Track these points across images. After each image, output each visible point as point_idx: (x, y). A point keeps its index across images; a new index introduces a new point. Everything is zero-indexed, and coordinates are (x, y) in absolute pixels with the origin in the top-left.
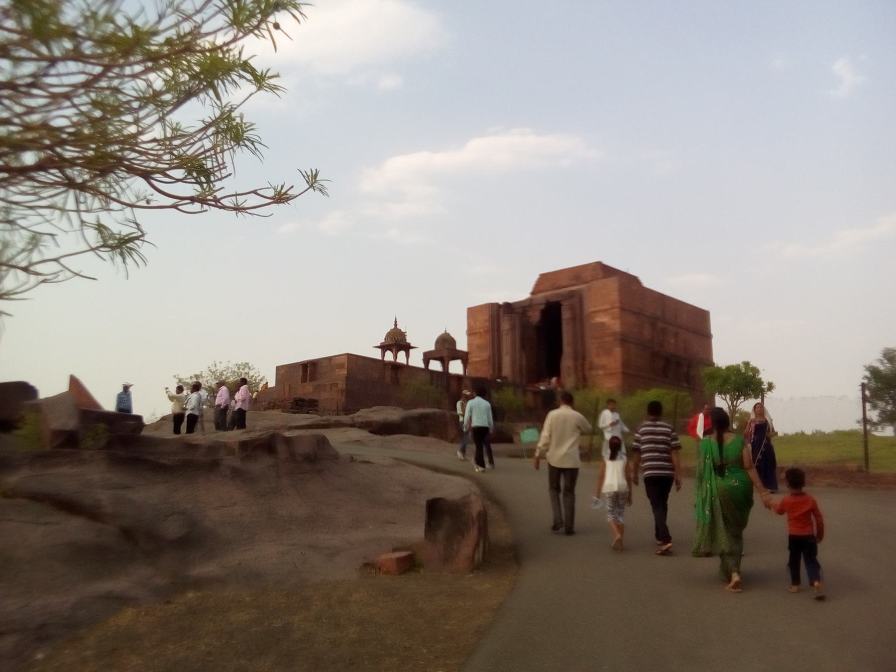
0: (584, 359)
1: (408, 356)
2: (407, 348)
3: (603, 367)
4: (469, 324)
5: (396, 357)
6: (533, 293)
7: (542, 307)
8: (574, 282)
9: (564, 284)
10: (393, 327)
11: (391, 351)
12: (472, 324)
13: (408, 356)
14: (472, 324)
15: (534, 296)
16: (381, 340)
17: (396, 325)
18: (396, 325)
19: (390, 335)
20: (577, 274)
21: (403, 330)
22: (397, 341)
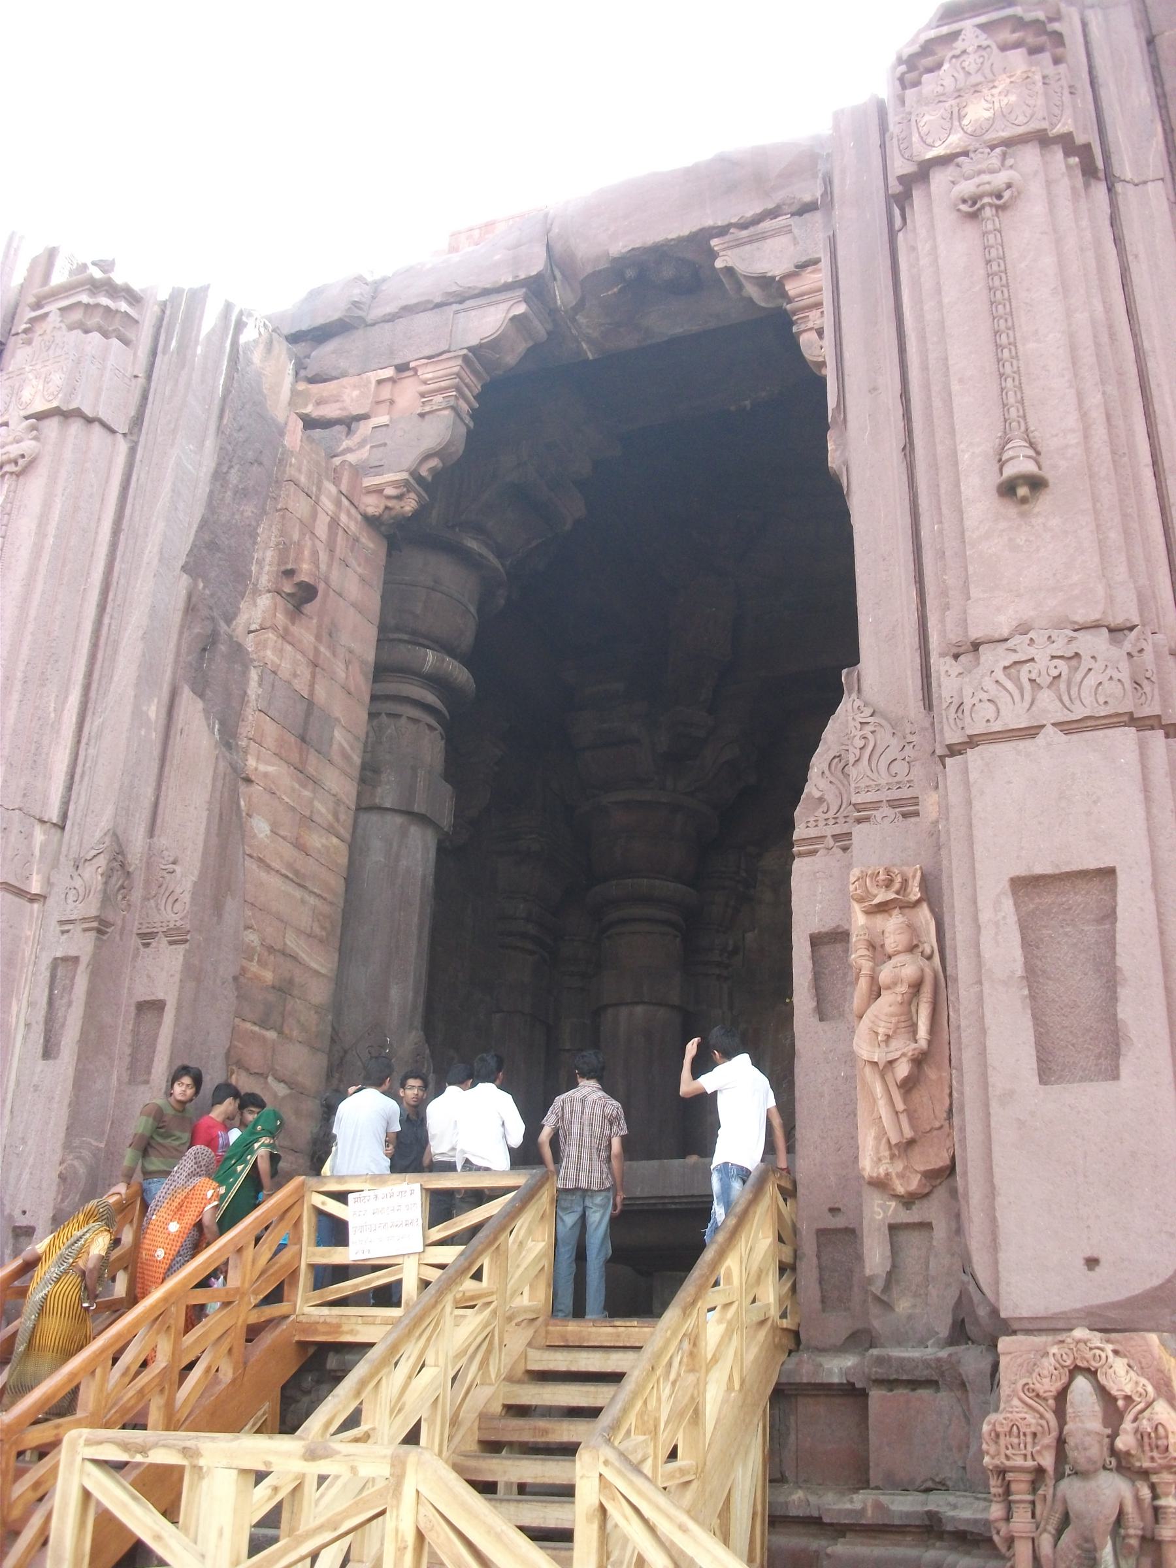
7: (487, 322)
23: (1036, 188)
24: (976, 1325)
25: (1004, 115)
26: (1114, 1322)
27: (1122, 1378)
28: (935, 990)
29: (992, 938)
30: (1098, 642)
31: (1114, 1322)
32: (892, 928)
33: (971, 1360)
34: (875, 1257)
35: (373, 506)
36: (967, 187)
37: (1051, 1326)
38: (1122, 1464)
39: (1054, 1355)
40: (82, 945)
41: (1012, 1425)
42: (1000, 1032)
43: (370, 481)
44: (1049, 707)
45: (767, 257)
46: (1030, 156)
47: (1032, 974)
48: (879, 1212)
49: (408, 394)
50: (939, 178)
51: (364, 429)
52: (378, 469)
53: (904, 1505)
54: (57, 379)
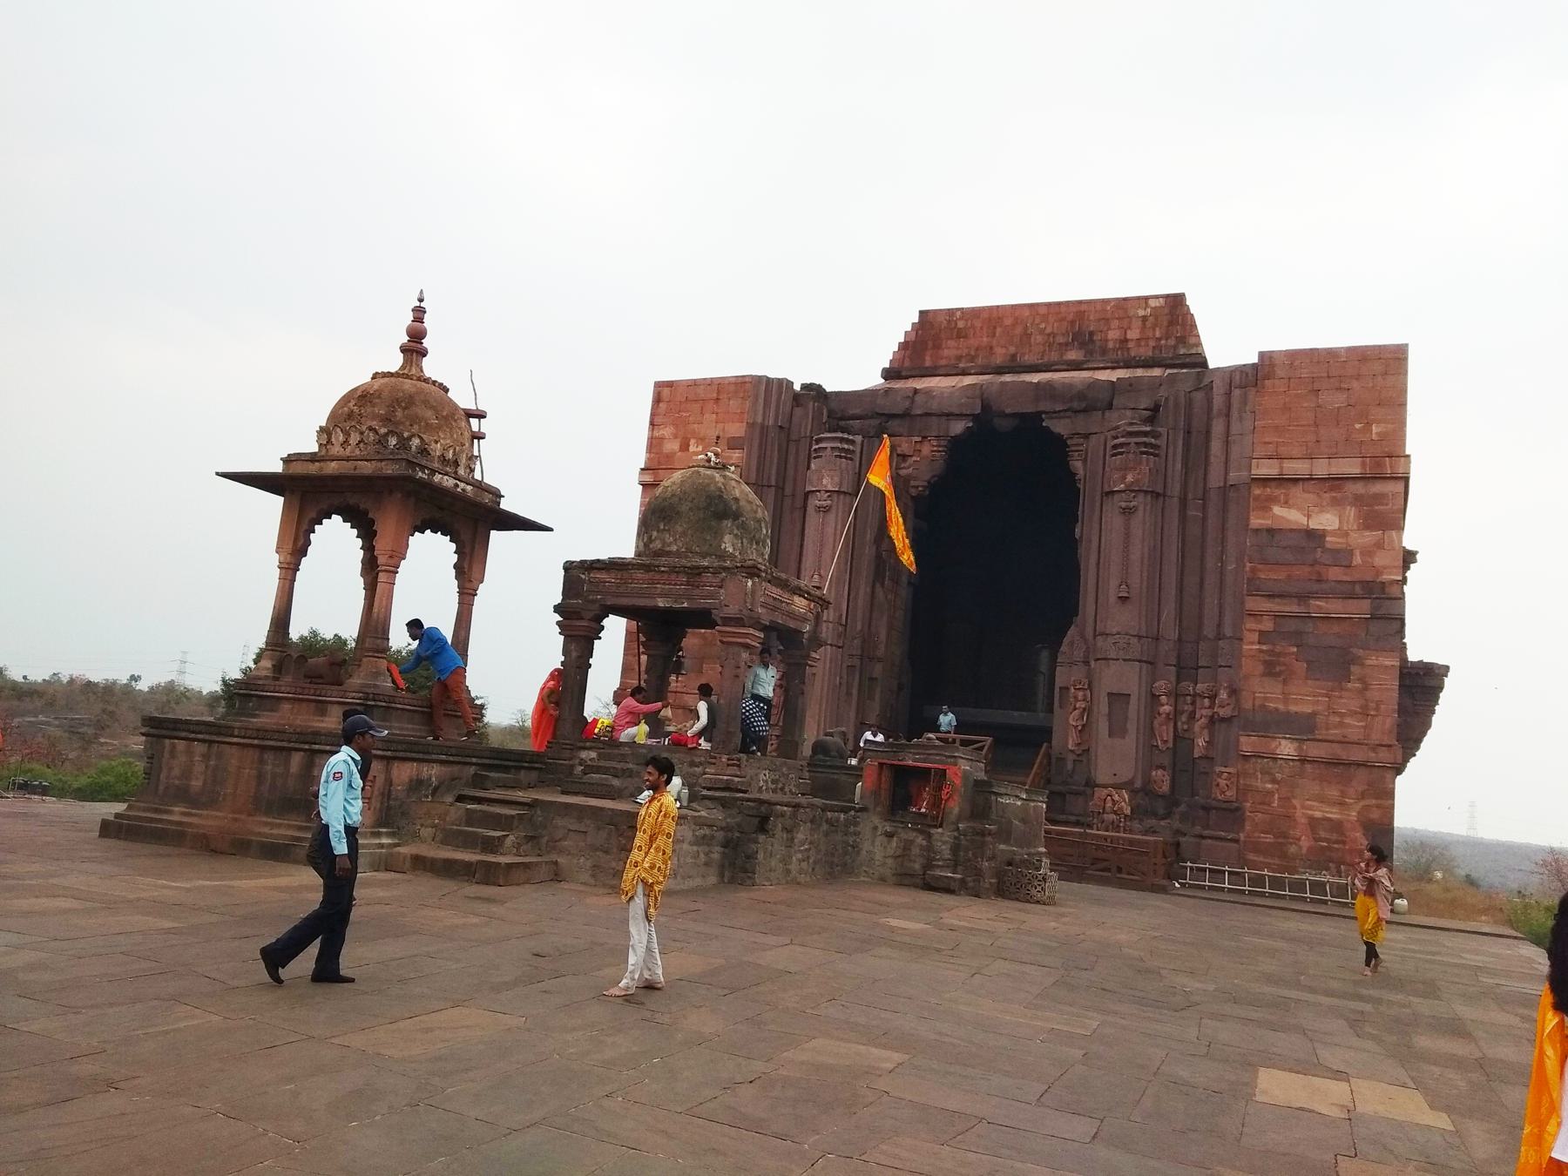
0: (1186, 669)
1: (469, 573)
2: (474, 519)
3: (1302, 727)
4: (654, 444)
5: (377, 571)
6: (888, 374)
7: (958, 427)
8: (1073, 355)
9: (1029, 359)
10: (394, 362)
11: (356, 517)
12: (672, 446)
13: (469, 573)
14: (672, 446)
15: (898, 385)
16: (294, 431)
17: (414, 348)
18: (414, 348)
19: (353, 411)
20: (1081, 328)
21: (461, 397)
22: (392, 467)
23: (1141, 508)
24: (1091, 784)
25: (1137, 481)
26: (1117, 787)
27: (1116, 797)
28: (1088, 711)
29: (1103, 706)
30: (1134, 641)
31: (1117, 787)
32: (1080, 694)
33: (1089, 791)
34: (1070, 766)
35: (913, 492)
36: (1123, 504)
37: (1105, 786)
38: (1115, 813)
39: (1106, 791)
40: (857, 662)
41: (1093, 805)
42: (1103, 727)
43: (913, 483)
44: (1122, 654)
45: (1060, 427)
46: (1141, 497)
47: (1110, 715)
48: (1071, 757)
49: (926, 449)
50: (1116, 496)
51: (911, 461)
52: (915, 479)
53: (1073, 818)
54: (837, 479)
